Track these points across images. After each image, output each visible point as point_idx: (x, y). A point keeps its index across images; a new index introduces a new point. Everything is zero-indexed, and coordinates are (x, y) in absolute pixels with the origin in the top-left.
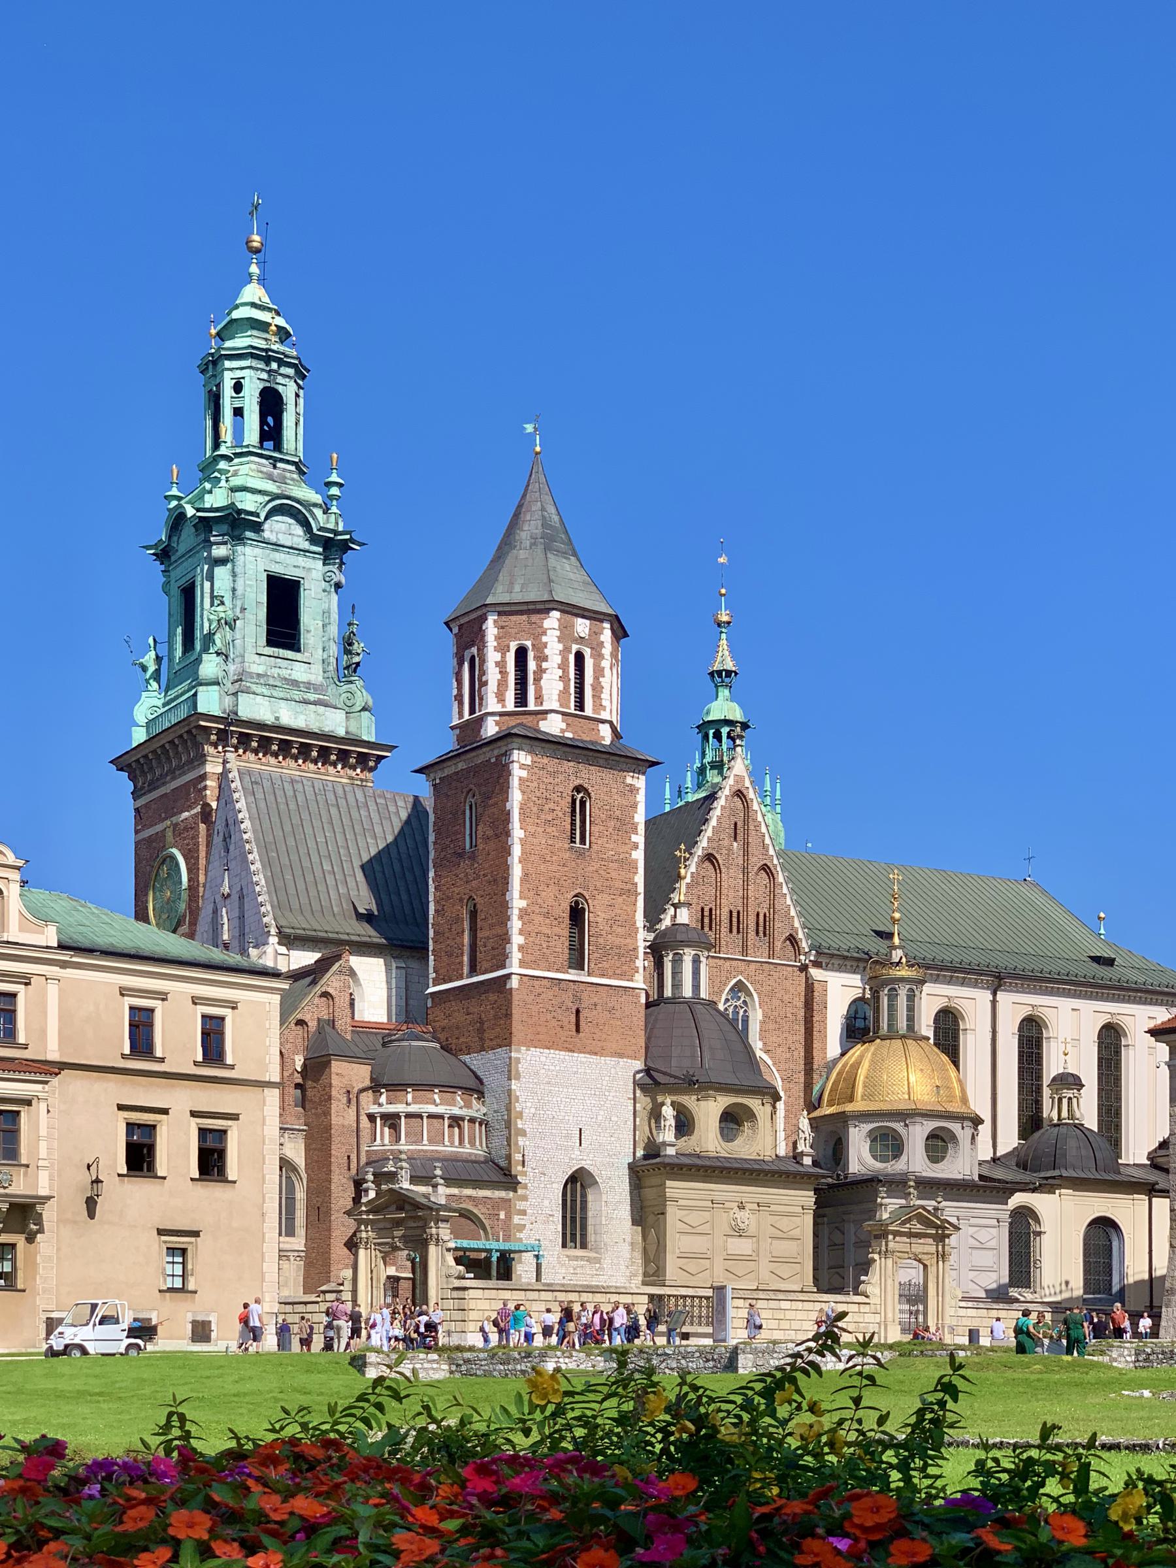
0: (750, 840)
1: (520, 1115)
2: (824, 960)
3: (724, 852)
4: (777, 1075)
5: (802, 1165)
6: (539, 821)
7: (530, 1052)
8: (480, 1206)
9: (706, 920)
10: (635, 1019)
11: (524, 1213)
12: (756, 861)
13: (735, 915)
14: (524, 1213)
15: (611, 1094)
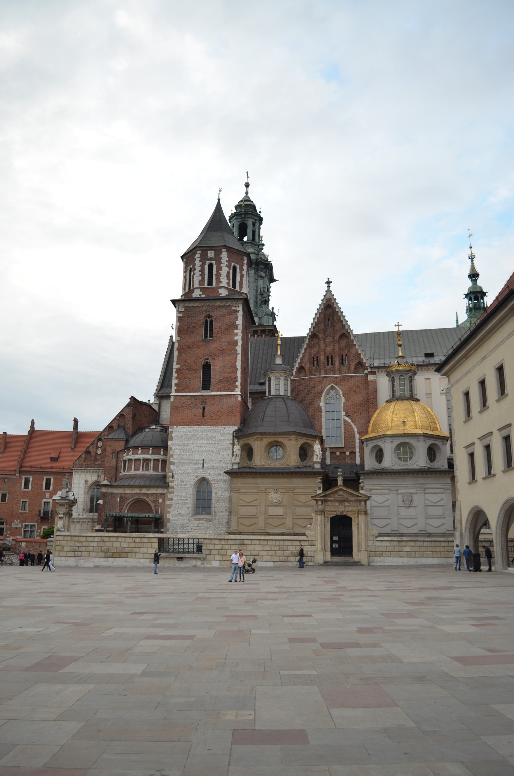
0: (335, 325)
1: (172, 456)
2: (376, 370)
3: (322, 331)
4: (354, 426)
5: (313, 468)
6: (187, 332)
7: (178, 428)
8: (150, 497)
9: (315, 362)
10: (234, 408)
11: (172, 499)
12: (338, 333)
13: (330, 357)
14: (172, 499)
15: (221, 443)
